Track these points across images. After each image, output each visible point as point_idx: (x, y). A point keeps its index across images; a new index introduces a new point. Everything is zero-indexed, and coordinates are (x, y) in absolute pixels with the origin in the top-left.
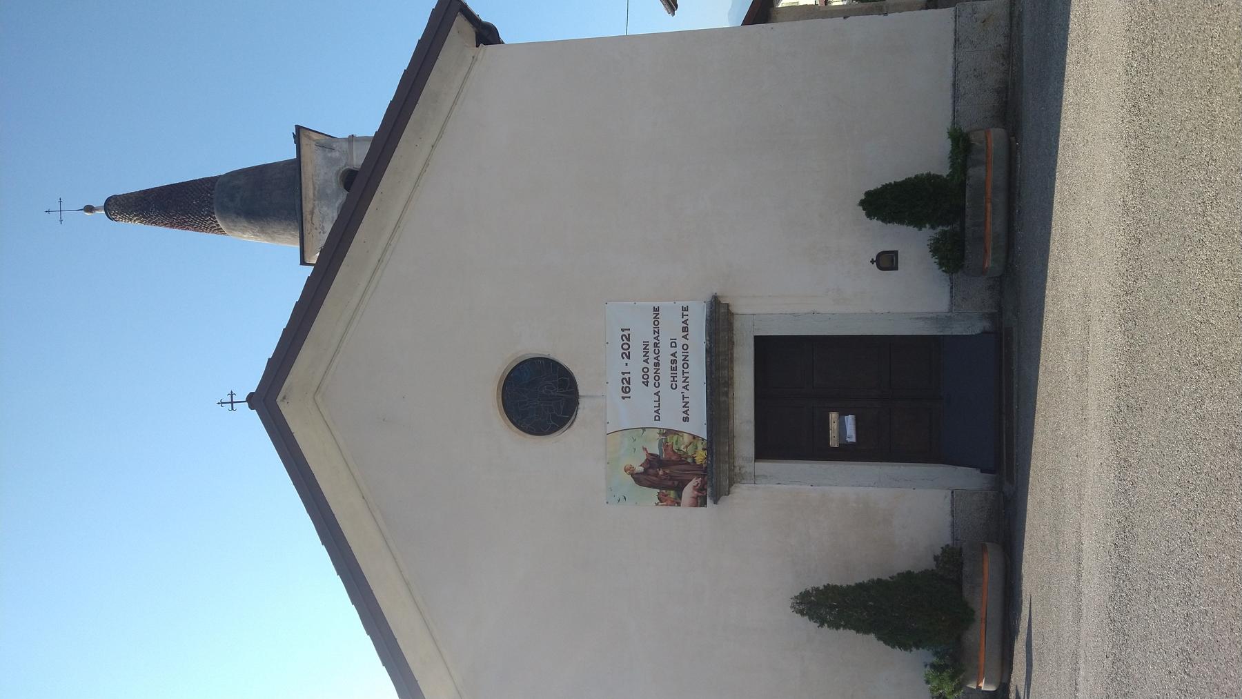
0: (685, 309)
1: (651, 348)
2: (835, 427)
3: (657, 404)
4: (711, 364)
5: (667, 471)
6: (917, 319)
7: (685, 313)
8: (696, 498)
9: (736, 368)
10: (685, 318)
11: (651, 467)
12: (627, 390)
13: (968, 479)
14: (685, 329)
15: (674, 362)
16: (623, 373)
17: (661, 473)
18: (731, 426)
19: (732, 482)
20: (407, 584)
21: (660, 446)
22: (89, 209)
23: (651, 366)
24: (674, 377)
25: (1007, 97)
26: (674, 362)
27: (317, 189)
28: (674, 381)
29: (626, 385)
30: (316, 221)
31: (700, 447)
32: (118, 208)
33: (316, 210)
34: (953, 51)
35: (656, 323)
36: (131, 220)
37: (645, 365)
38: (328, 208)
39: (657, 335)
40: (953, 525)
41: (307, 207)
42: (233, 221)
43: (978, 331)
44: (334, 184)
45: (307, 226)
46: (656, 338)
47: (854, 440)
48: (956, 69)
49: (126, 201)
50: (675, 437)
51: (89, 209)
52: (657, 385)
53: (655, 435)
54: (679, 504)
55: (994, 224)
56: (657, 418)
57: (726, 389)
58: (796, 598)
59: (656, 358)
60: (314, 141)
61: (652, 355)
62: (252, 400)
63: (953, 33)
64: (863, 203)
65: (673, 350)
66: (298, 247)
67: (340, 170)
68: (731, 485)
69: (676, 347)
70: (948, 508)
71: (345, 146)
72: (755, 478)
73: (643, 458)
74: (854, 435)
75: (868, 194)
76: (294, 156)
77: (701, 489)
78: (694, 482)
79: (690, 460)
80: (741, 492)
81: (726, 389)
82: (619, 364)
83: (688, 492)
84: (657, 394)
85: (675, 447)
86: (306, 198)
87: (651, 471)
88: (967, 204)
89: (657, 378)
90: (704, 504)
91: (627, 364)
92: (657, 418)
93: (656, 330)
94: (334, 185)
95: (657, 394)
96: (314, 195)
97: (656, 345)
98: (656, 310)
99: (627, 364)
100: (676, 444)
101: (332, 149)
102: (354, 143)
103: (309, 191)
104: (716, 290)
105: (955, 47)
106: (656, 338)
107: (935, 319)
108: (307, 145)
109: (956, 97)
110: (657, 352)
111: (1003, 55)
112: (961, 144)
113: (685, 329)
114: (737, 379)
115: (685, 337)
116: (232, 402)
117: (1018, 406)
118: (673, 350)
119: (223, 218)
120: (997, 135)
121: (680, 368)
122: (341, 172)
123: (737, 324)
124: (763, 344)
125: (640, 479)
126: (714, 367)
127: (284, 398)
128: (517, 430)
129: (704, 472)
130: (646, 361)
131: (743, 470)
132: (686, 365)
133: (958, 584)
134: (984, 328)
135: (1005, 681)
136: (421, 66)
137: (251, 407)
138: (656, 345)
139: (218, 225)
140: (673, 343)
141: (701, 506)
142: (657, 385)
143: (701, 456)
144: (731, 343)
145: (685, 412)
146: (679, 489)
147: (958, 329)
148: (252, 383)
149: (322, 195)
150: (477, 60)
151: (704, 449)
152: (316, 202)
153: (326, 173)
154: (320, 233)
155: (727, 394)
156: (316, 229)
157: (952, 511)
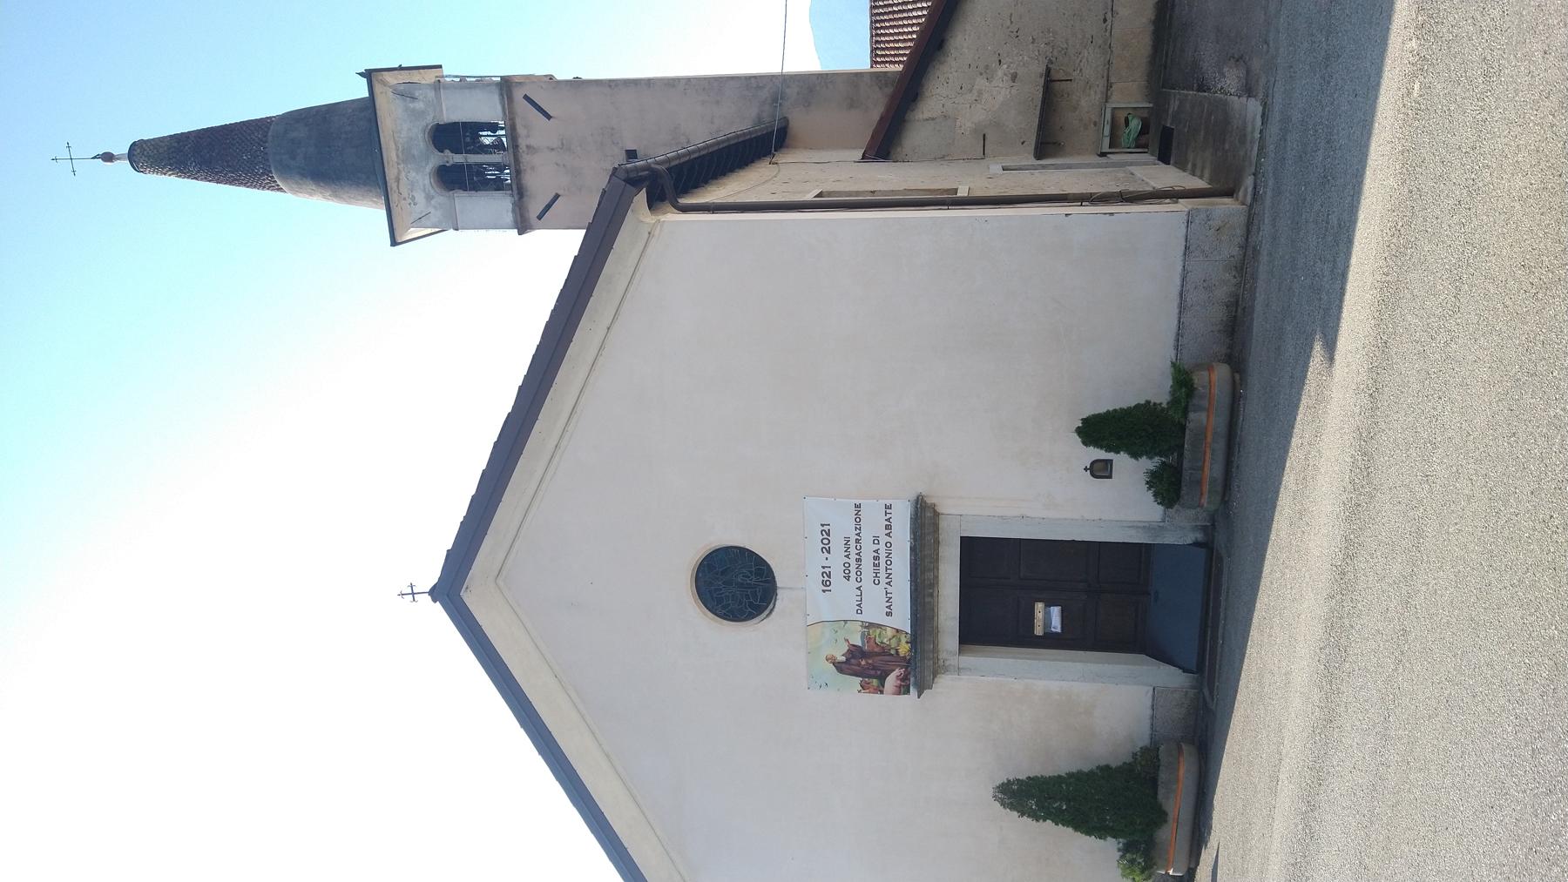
0: (888, 507)
1: (852, 543)
2: (1041, 617)
3: (859, 598)
4: (916, 590)
5: (870, 661)
6: (1129, 527)
7: (888, 511)
8: (900, 687)
9: (941, 567)
10: (888, 516)
11: (853, 657)
12: (828, 583)
13: (1170, 677)
14: (888, 527)
15: (876, 558)
16: (823, 567)
17: (863, 663)
18: (935, 624)
19: (935, 674)
20: (608, 756)
21: (863, 634)
22: (108, 157)
23: (852, 561)
24: (876, 573)
25: (1236, 311)
26: (876, 558)
27: (400, 150)
28: (876, 576)
29: (826, 578)
30: (405, 191)
31: (904, 640)
32: (146, 159)
33: (403, 175)
34: (1182, 258)
35: (858, 520)
36: (165, 174)
37: (847, 560)
38: (417, 173)
39: (858, 531)
40: (1152, 717)
41: (391, 173)
42: (297, 183)
43: (1189, 541)
44: (421, 143)
45: (394, 197)
46: (858, 534)
47: (1059, 630)
48: (1183, 279)
49: (155, 151)
50: (878, 631)
51: (108, 157)
52: (859, 580)
53: (858, 627)
54: (882, 692)
55: (1212, 469)
56: (859, 611)
57: (931, 591)
58: (998, 787)
59: (858, 554)
60: (390, 87)
61: (853, 551)
62: (435, 593)
63: (1183, 240)
64: (1079, 431)
65: (876, 547)
66: (383, 213)
67: (427, 126)
68: (934, 677)
69: (879, 544)
70: (1149, 703)
71: (431, 94)
72: (959, 670)
73: (845, 648)
74: (1059, 626)
75: (1085, 421)
76: (366, 94)
77: (904, 679)
78: (897, 672)
79: (893, 652)
80: (944, 683)
81: (931, 591)
82: (821, 558)
83: (891, 681)
84: (859, 588)
85: (878, 640)
86: (388, 163)
87: (853, 661)
88: (1186, 446)
89: (859, 573)
90: (907, 692)
91: (827, 559)
92: (859, 611)
93: (858, 527)
94: (422, 145)
95: (859, 588)
96: (398, 156)
97: (857, 541)
98: (858, 506)
99: (827, 559)
100: (879, 637)
101: (414, 98)
102: (442, 91)
103: (391, 154)
104: (922, 488)
105: (1185, 254)
106: (858, 534)
107: (1147, 528)
108: (381, 93)
109: (1182, 308)
110: (858, 548)
111: (1236, 267)
112: (1183, 381)
113: (888, 527)
114: (942, 577)
115: (888, 535)
116: (413, 594)
117: (1225, 621)
118: (876, 547)
119: (284, 179)
120: (1222, 372)
121: (883, 565)
122: (429, 127)
123: (943, 524)
124: (968, 544)
125: (841, 667)
126: (919, 571)
127: (467, 588)
128: (713, 616)
129: (908, 664)
130: (847, 556)
131: (947, 663)
132: (889, 562)
133: (1154, 783)
134: (1196, 538)
135: (1192, 866)
136: (594, 258)
137: (435, 600)
138: (857, 541)
139: (278, 185)
140: (876, 540)
141: (904, 694)
142: (859, 580)
143: (904, 649)
144: (937, 542)
145: (889, 607)
146: (882, 679)
147: (1169, 539)
148: (431, 574)
149: (407, 157)
150: (653, 236)
151: (907, 643)
152: (401, 166)
153: (410, 129)
154: (410, 204)
155: (931, 595)
156: (405, 199)
157: (1153, 706)
